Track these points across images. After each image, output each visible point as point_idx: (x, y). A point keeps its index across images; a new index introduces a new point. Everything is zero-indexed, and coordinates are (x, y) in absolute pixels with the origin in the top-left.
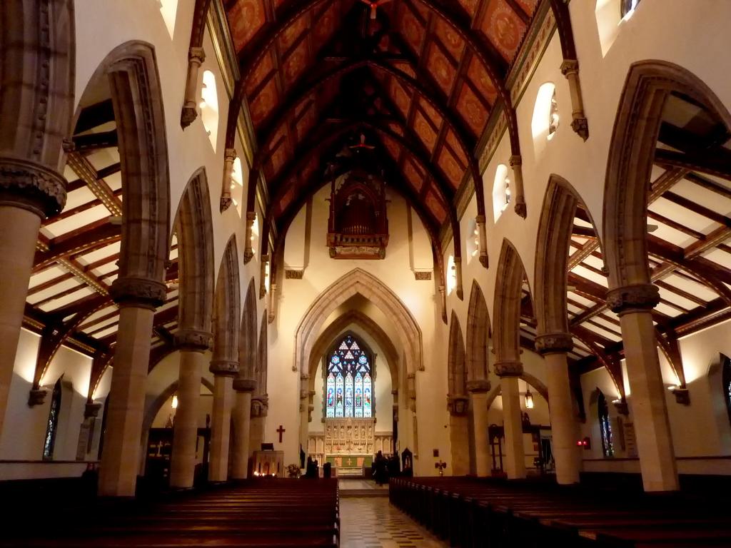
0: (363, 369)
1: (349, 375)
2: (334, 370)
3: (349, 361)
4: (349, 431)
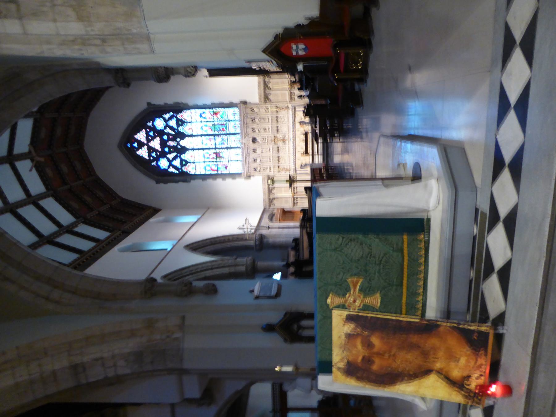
0: (173, 123)
1: (183, 143)
2: (179, 166)
3: (163, 144)
4: (259, 139)
